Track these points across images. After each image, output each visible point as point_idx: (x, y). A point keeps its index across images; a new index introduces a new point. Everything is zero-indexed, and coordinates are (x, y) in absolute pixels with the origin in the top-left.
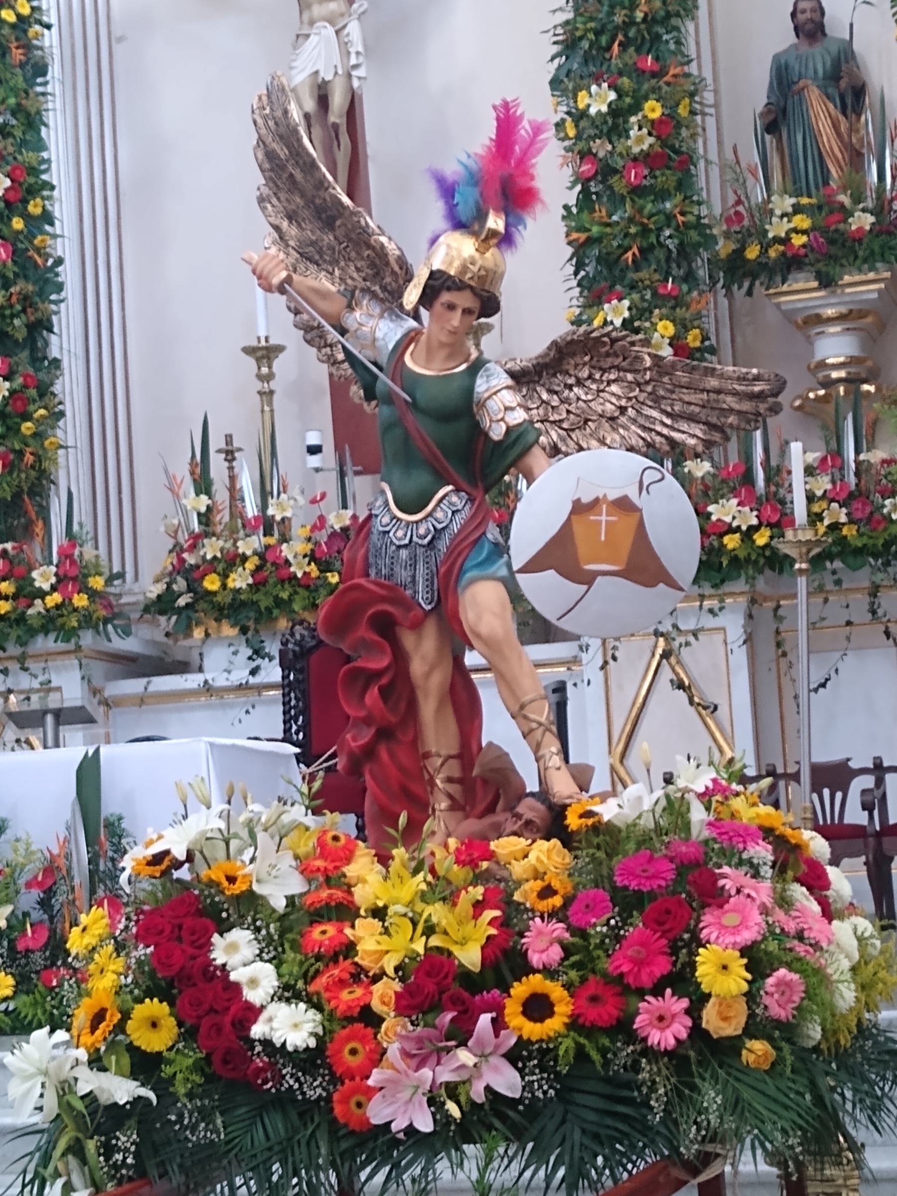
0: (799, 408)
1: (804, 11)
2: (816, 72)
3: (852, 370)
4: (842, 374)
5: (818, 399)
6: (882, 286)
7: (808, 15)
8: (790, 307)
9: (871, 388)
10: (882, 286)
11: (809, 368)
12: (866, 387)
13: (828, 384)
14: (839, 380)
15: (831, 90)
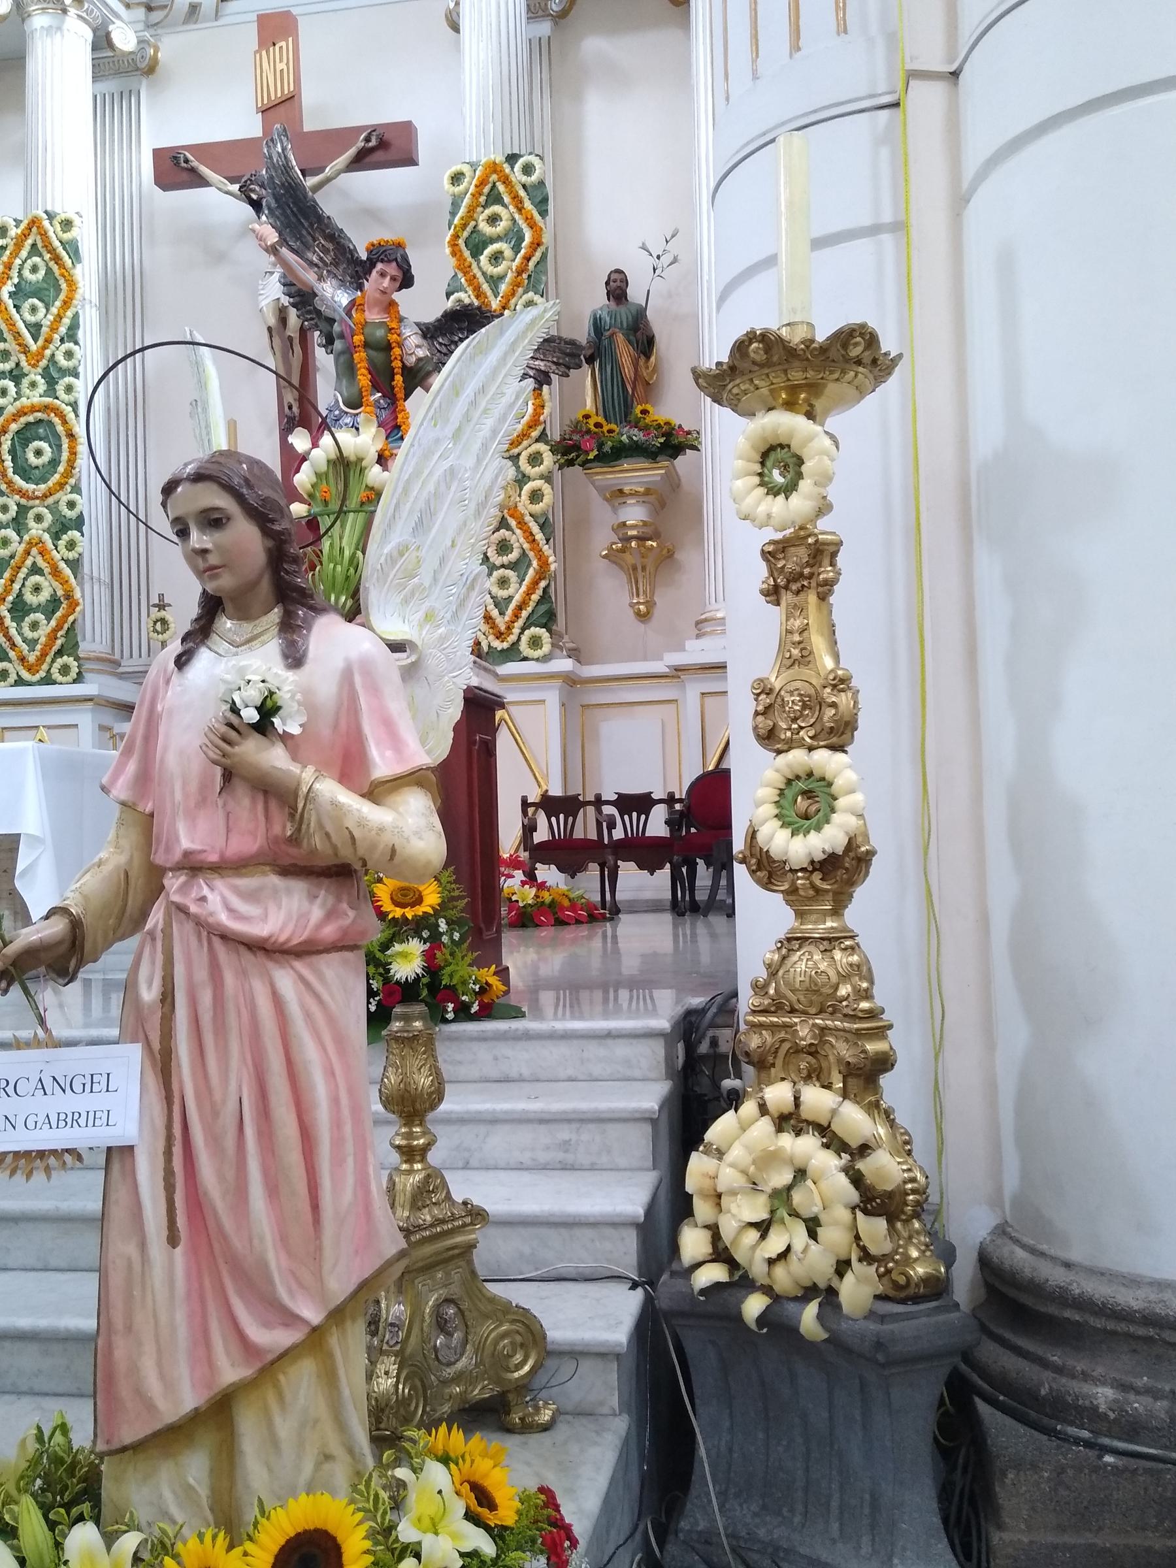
0: (605, 557)
1: (615, 281)
2: (621, 322)
3: (645, 530)
4: (634, 533)
5: (617, 550)
6: (663, 472)
7: (618, 284)
8: (604, 483)
9: (654, 544)
10: (663, 472)
11: (613, 529)
12: (650, 543)
13: (627, 539)
14: (633, 537)
15: (632, 338)
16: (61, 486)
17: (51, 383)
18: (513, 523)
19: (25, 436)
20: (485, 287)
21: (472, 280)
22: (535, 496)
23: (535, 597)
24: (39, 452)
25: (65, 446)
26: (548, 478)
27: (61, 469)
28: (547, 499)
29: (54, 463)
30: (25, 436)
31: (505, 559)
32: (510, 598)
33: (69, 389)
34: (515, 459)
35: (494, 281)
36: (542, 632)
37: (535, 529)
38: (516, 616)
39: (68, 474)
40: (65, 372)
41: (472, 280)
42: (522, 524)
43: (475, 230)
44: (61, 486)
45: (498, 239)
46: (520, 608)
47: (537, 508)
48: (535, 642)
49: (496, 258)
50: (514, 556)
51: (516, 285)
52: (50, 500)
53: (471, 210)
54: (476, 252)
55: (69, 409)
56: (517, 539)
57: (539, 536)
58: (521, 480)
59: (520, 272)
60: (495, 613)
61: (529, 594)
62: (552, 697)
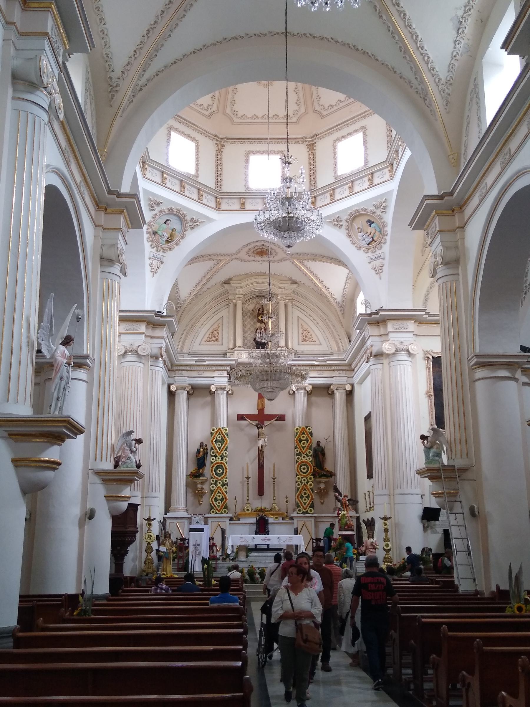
16: (224, 477)
17: (222, 458)
18: (307, 489)
19: (217, 468)
20: (302, 448)
21: (300, 447)
22: (311, 485)
23: (311, 503)
24: (219, 471)
25: (225, 470)
26: (312, 482)
27: (224, 474)
28: (313, 485)
29: (223, 473)
30: (217, 468)
31: (305, 496)
32: (306, 503)
33: (225, 460)
34: (307, 478)
35: (303, 447)
36: (312, 509)
37: (311, 491)
38: (308, 506)
39: (225, 475)
40: (225, 457)
41: (300, 447)
42: (308, 490)
43: (300, 439)
44: (224, 477)
45: (304, 440)
46: (308, 504)
47: (311, 487)
48: (311, 511)
49: (304, 444)
50: (307, 495)
51: (307, 448)
52: (222, 480)
53: (299, 436)
54: (300, 442)
55: (225, 463)
56: (307, 492)
57: (311, 492)
58: (308, 482)
59: (308, 447)
60: (304, 505)
61: (310, 502)
62: (313, 520)
